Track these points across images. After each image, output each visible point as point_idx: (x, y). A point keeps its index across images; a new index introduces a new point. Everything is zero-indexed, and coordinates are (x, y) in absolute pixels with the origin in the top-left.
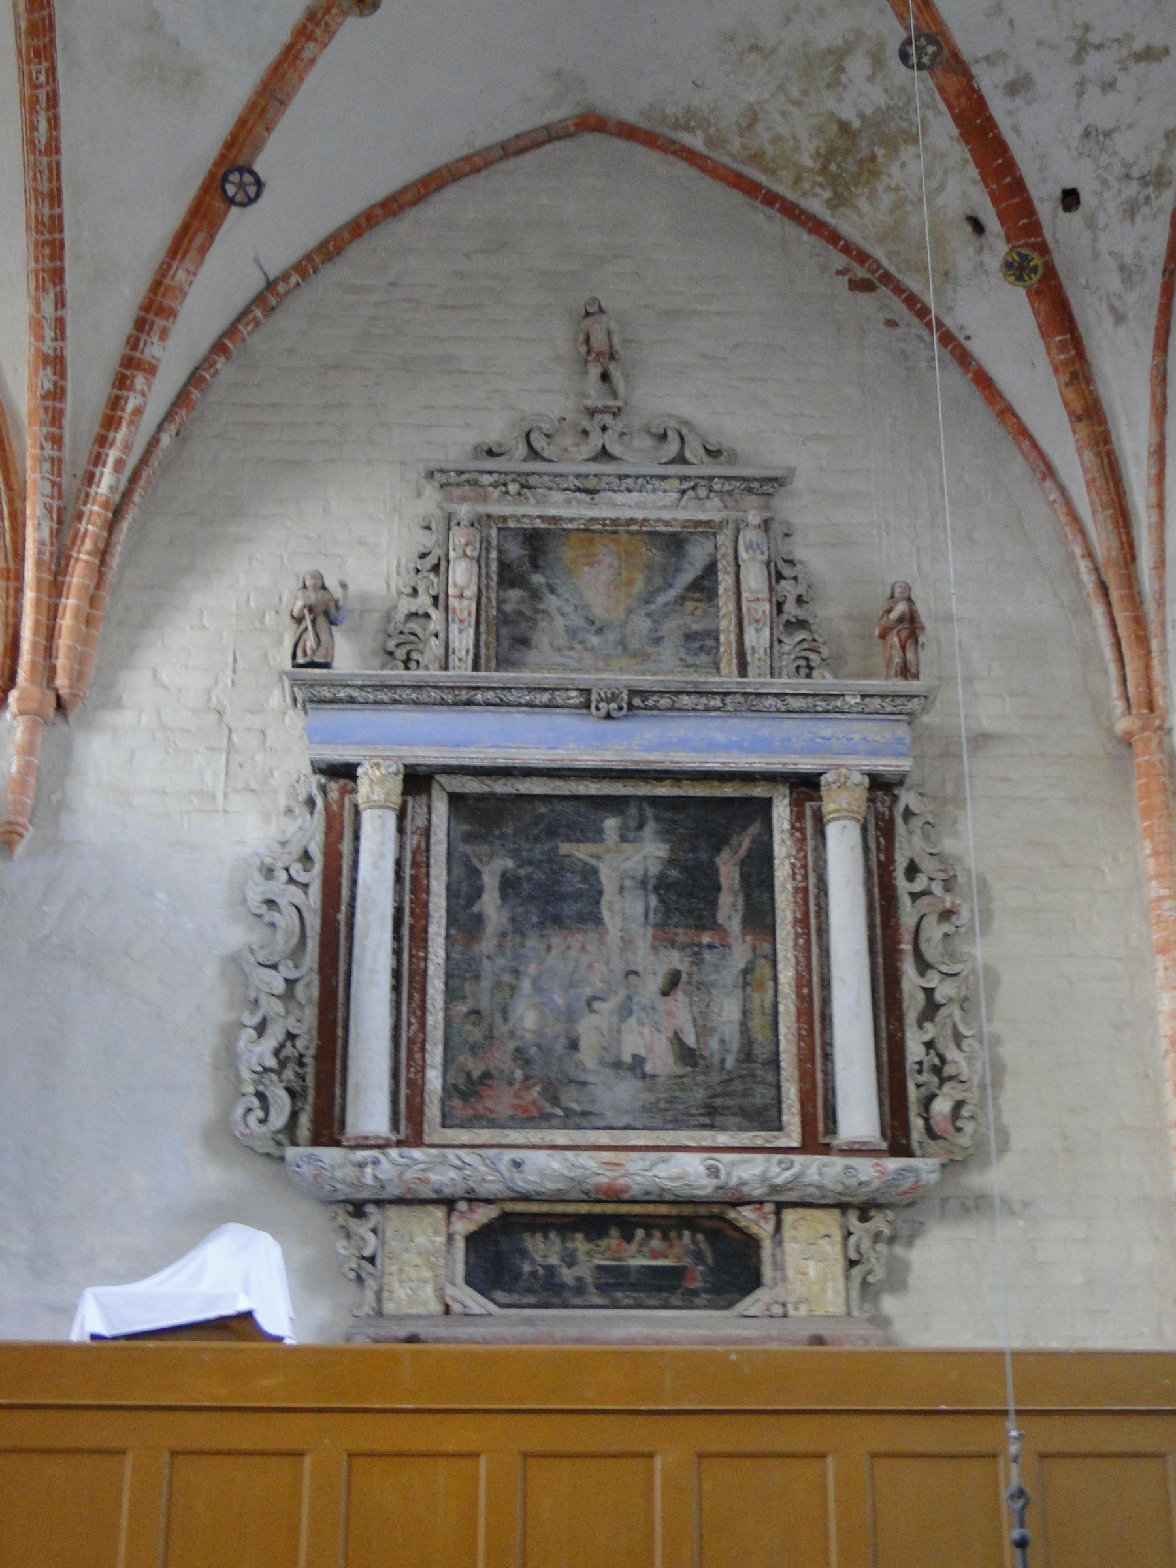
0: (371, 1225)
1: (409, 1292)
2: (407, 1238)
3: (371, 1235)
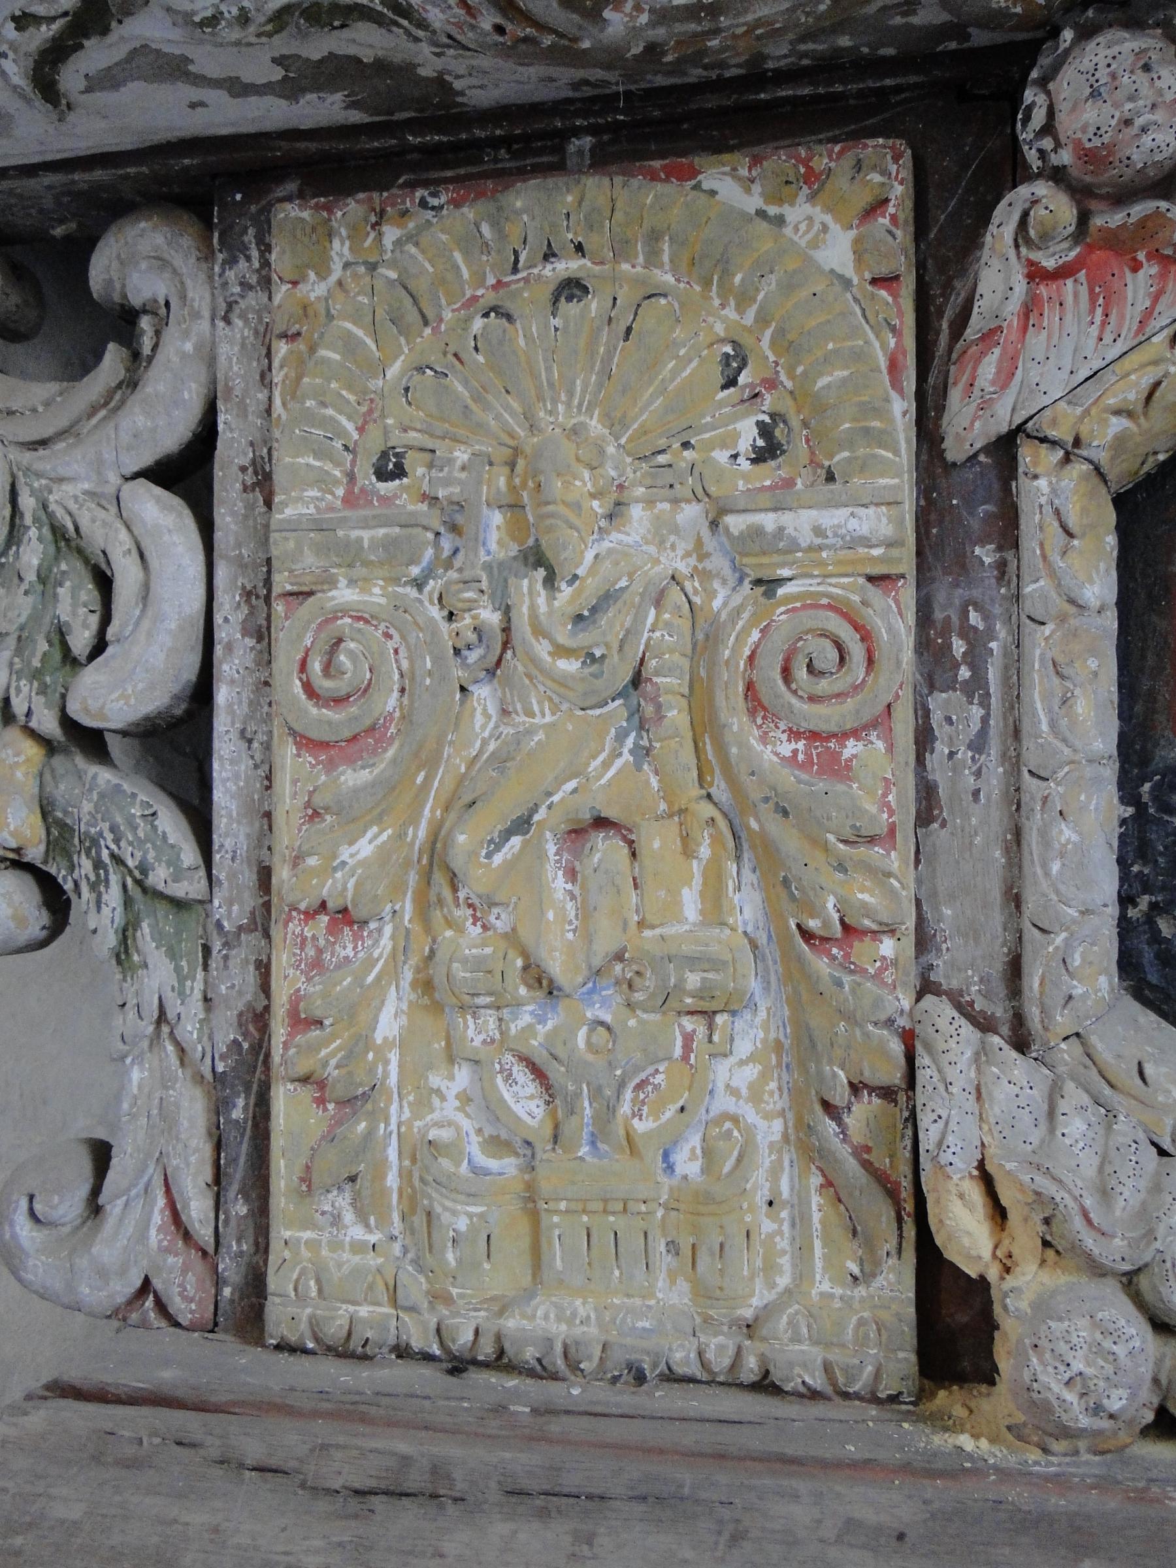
0: (159, 420)
1: (524, 1103)
2: (494, 534)
3: (161, 513)
